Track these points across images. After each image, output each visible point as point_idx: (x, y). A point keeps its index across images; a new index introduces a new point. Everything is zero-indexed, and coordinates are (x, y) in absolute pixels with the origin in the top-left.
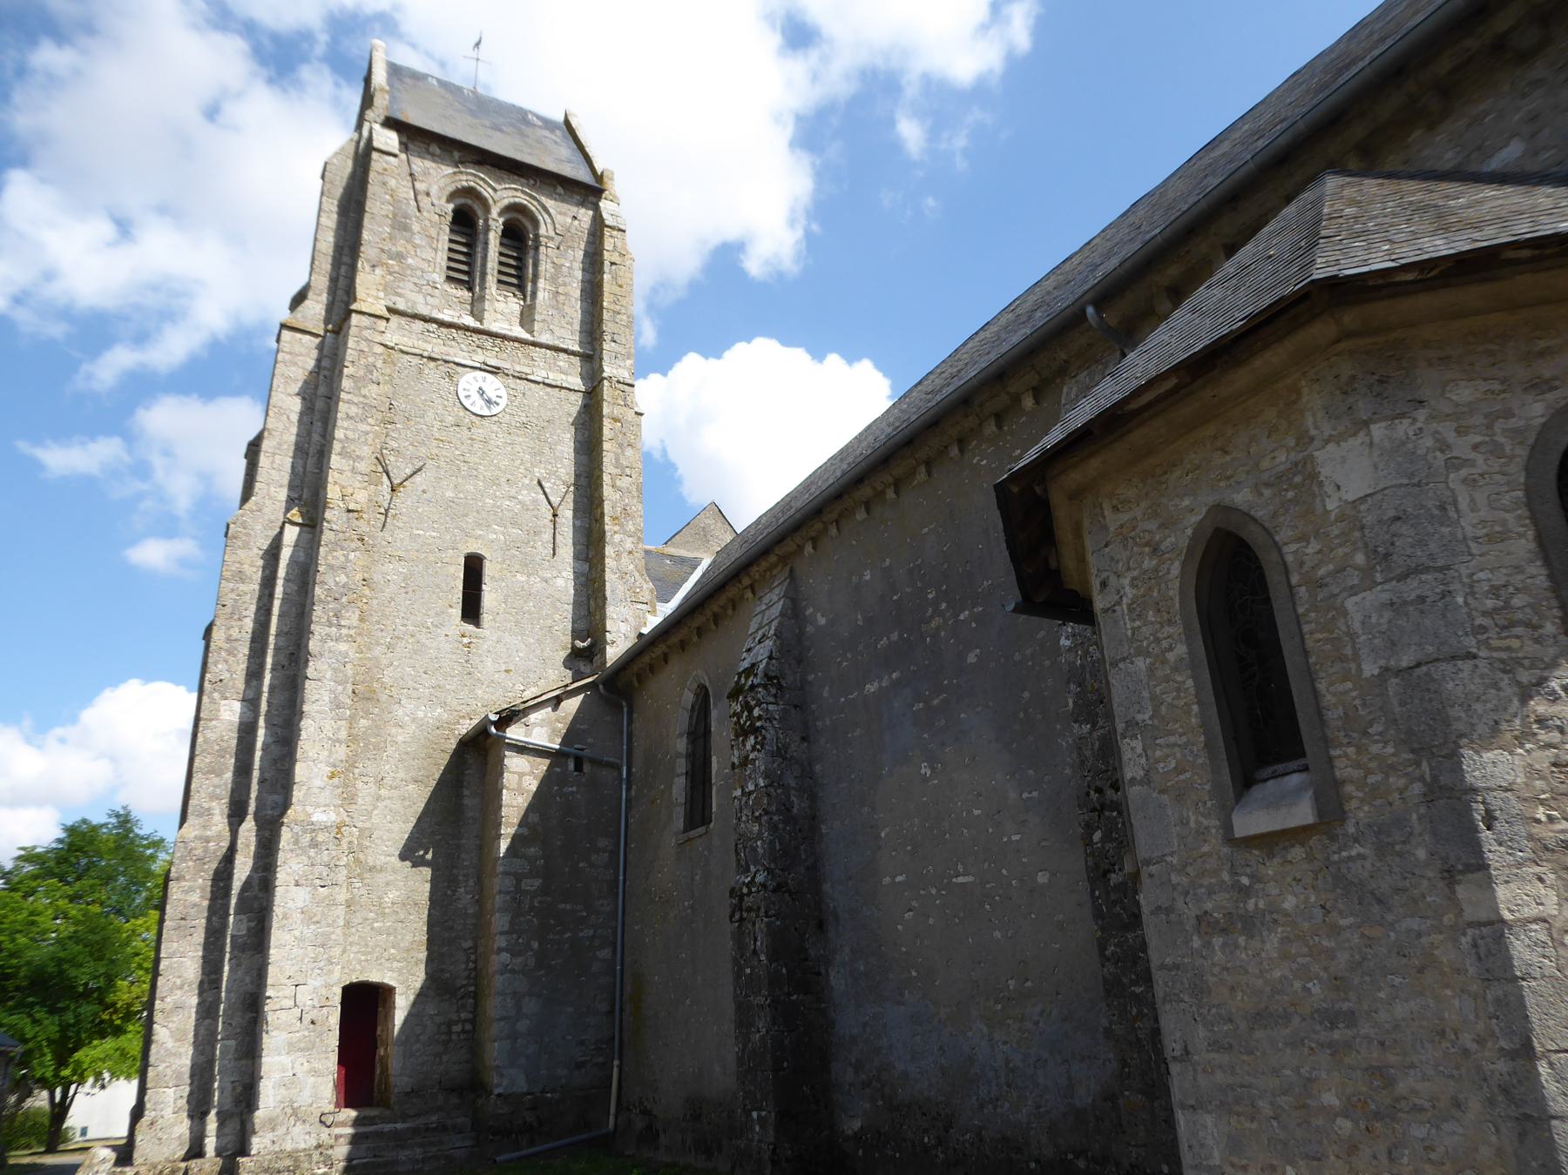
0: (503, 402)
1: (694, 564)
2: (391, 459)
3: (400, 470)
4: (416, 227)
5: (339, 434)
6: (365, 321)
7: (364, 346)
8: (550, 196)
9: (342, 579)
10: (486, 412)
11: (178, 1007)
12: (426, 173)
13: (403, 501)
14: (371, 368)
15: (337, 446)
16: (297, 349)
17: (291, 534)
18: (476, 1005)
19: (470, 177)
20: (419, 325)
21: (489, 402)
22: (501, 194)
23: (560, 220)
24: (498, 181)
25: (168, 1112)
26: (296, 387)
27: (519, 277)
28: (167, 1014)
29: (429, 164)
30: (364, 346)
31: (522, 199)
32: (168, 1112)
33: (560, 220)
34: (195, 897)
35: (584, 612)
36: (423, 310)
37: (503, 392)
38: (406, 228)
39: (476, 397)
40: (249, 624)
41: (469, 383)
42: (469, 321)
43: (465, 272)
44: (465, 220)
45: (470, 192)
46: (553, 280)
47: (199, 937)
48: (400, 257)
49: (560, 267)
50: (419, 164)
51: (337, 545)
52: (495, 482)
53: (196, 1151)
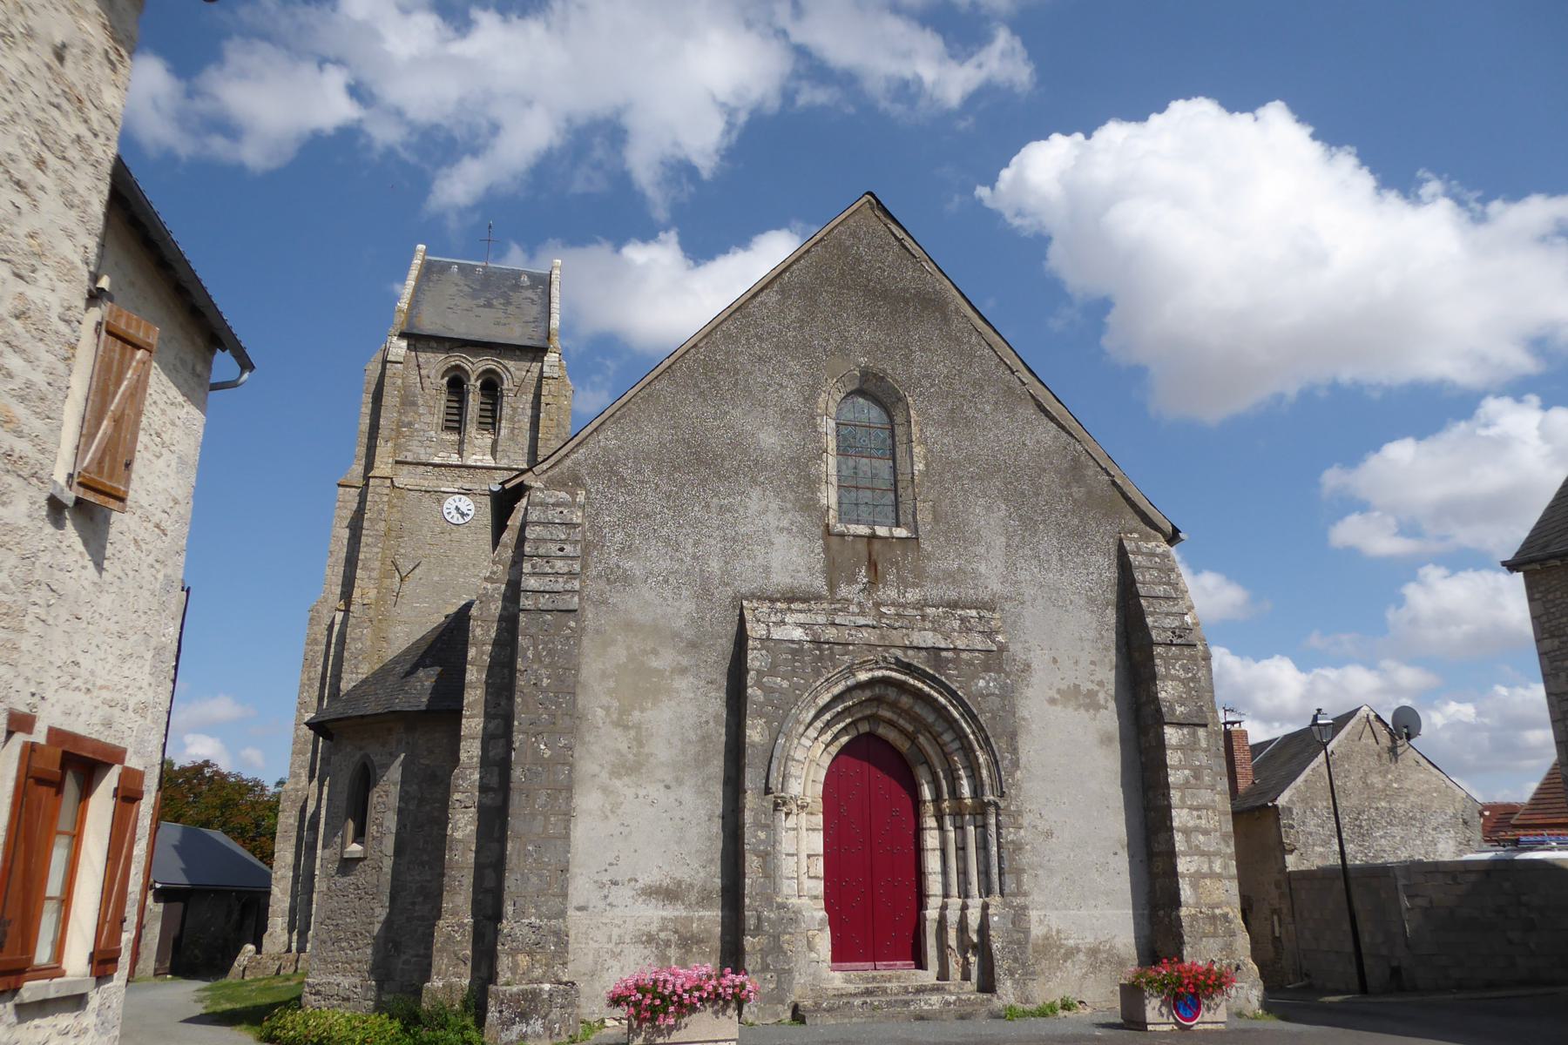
0: (472, 513)
1: (324, 847)
2: (400, 562)
3: (405, 567)
4: (420, 402)
5: (361, 556)
6: (378, 481)
7: (377, 498)
8: (511, 359)
9: (359, 645)
10: (461, 521)
11: (283, 877)
12: (428, 362)
13: (408, 587)
14: (380, 512)
15: (360, 564)
16: (348, 498)
17: (339, 616)
18: (570, 771)
19: (456, 359)
20: (421, 468)
21: (463, 515)
22: (475, 366)
23: (514, 372)
24: (474, 356)
25: (278, 930)
26: (346, 523)
27: (491, 420)
28: (278, 881)
29: (429, 355)
30: (377, 498)
31: (492, 365)
32: (278, 930)
33: (514, 372)
34: (291, 821)
35: (174, 932)
36: (424, 458)
37: (472, 507)
38: (414, 404)
39: (454, 512)
40: (320, 669)
41: (450, 504)
42: (455, 459)
43: (455, 423)
44: (456, 384)
45: (458, 367)
46: (512, 420)
47: (294, 841)
48: (410, 424)
49: (516, 406)
50: (423, 357)
51: (358, 625)
52: (465, 567)
53: (289, 950)
